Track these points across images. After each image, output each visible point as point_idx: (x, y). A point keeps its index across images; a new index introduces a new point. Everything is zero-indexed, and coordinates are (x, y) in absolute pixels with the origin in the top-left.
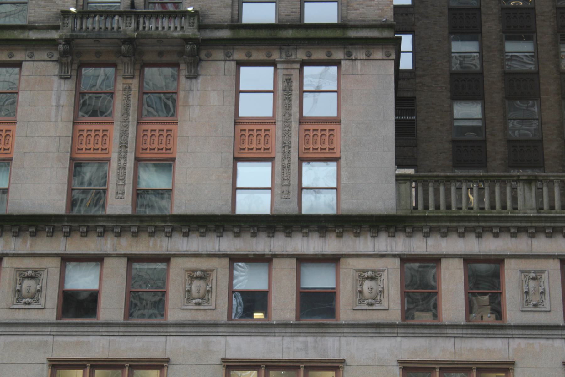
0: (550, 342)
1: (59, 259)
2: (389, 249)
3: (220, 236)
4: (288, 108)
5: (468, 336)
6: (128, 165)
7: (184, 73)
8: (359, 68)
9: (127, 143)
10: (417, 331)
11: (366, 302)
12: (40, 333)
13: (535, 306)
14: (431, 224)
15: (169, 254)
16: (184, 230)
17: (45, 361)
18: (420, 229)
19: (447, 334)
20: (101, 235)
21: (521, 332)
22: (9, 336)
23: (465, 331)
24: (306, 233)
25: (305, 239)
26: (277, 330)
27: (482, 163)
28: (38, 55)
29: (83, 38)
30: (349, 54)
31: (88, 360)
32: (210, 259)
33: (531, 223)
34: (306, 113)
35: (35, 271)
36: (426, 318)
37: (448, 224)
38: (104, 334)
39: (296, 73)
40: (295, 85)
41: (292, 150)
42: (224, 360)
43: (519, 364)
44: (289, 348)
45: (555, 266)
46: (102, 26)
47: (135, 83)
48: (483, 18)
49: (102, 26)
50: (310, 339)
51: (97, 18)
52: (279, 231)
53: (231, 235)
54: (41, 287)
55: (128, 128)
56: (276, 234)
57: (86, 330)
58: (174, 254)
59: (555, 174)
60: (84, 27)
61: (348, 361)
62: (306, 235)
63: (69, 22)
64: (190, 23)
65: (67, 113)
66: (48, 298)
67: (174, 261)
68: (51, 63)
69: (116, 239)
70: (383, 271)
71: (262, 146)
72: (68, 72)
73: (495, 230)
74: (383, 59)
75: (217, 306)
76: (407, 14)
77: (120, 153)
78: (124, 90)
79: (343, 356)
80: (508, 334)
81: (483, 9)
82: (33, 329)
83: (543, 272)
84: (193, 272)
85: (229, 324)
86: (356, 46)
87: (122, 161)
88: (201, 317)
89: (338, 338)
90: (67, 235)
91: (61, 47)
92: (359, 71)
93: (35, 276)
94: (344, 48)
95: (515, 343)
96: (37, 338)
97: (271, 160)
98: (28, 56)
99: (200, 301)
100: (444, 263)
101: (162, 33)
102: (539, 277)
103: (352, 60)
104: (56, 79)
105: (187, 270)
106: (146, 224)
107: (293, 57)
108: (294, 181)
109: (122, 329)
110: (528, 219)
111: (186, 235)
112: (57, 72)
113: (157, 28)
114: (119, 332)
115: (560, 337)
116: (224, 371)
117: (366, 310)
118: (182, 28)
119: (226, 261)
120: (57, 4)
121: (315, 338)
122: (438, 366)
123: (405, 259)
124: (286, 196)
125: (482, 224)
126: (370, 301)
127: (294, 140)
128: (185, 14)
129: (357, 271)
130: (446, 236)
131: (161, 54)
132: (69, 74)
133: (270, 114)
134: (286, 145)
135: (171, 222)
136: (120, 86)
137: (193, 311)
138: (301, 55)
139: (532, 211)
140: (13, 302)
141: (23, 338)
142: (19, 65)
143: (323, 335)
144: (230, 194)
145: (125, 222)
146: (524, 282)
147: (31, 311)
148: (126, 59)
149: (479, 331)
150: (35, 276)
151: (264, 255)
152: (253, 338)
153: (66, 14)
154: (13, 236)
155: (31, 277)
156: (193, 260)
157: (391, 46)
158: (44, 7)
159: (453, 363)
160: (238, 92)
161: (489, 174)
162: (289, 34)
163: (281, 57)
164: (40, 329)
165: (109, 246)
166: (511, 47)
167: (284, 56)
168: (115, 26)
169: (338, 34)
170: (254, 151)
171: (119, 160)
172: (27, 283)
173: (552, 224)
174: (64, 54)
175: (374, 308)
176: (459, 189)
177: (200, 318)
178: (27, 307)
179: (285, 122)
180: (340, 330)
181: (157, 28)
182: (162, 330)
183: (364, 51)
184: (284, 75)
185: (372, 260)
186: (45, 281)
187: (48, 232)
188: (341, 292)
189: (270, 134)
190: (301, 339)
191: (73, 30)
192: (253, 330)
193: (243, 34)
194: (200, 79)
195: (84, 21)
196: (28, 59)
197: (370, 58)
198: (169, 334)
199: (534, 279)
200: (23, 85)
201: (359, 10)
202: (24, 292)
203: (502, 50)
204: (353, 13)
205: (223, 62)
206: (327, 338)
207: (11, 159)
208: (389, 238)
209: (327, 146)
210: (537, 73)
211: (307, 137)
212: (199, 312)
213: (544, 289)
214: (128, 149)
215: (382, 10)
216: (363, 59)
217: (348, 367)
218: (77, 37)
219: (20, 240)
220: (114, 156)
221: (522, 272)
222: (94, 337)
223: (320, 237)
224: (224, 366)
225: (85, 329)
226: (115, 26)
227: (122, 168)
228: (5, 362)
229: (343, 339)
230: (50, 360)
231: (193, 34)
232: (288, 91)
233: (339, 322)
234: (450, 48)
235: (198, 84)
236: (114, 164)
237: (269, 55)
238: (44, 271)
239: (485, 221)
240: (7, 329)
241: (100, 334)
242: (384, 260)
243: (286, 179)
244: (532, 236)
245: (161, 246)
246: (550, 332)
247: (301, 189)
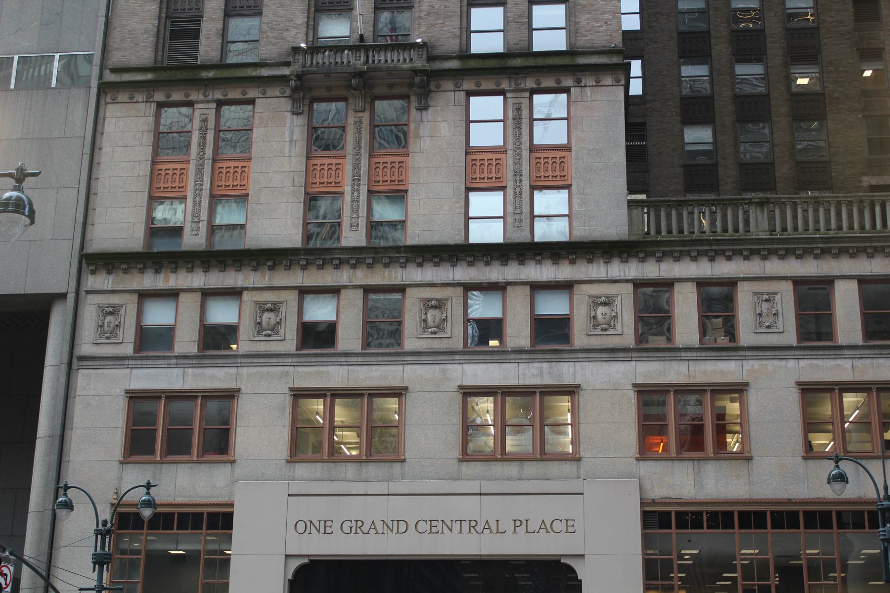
0: (784, 362)
1: (297, 291)
2: (622, 274)
3: (454, 265)
4: (518, 137)
5: (702, 358)
6: (361, 198)
7: (414, 104)
8: (589, 95)
9: (360, 176)
10: (651, 354)
11: (600, 327)
12: (281, 364)
13: (768, 327)
14: (664, 249)
15: (404, 285)
16: (418, 261)
17: (287, 391)
18: (653, 254)
19: (681, 357)
20: (337, 267)
21: (754, 353)
22: (251, 368)
23: (699, 354)
24: (539, 261)
25: (538, 266)
26: (512, 357)
27: (714, 187)
28: (271, 92)
29: (314, 73)
30: (578, 81)
31: (328, 389)
32: (444, 288)
33: (764, 245)
34: (536, 141)
35: (274, 304)
36: (660, 342)
37: (681, 248)
38: (342, 363)
39: (526, 102)
40: (525, 113)
41: (523, 178)
42: (461, 387)
43: (752, 385)
44: (524, 374)
45: (787, 288)
46: (332, 61)
47: (366, 116)
48: (713, 41)
49: (332, 61)
50: (545, 365)
51: (327, 53)
52: (512, 259)
53: (464, 264)
54: (281, 319)
55: (360, 161)
56: (509, 262)
57: (325, 360)
58: (409, 284)
59: (787, 196)
60: (314, 62)
61: (584, 386)
62: (539, 262)
63: (300, 58)
64: (419, 55)
65: (300, 148)
66: (287, 330)
67: (409, 291)
68: (283, 99)
69: (352, 270)
71: (493, 175)
72: (300, 108)
73: (728, 253)
74: (612, 85)
75: (453, 334)
76: (635, 40)
77: (353, 186)
78: (355, 123)
79: (578, 381)
80: (741, 356)
81: (712, 33)
82: (274, 360)
83: (776, 294)
84: (429, 301)
85: (465, 352)
86: (585, 73)
87: (356, 194)
88: (436, 345)
89: (573, 363)
90: (304, 268)
91: (293, 83)
92: (589, 97)
93: (274, 308)
94: (574, 75)
95: (748, 365)
96: (279, 368)
97: (503, 189)
98: (261, 93)
99: (436, 329)
100: (677, 287)
101: (391, 65)
102: (772, 299)
103: (581, 86)
104: (288, 115)
105: (422, 300)
106: (380, 255)
107: (522, 86)
108: (526, 209)
109: (360, 359)
110: (760, 241)
111: (420, 265)
112: (289, 108)
113: (386, 61)
114: (357, 362)
115: (793, 357)
116: (461, 398)
117: (600, 335)
118: (411, 60)
119: (460, 290)
120: (288, 41)
121: (550, 363)
122: (672, 389)
123: (638, 284)
124: (518, 224)
126: (604, 326)
127: (525, 168)
128: (414, 46)
129: (590, 296)
130: (679, 261)
131: (391, 86)
132: (302, 109)
133: (500, 143)
134: (518, 174)
135: (405, 253)
136: (351, 120)
137: (429, 340)
138: (530, 83)
139: (765, 234)
140: (254, 334)
141: (265, 369)
142: (252, 102)
143: (558, 361)
144: (463, 224)
145: (361, 254)
146: (757, 304)
147: (272, 342)
148: (357, 93)
149: (713, 354)
150: (274, 308)
151: (497, 283)
152: (488, 365)
153: (296, 50)
154: (252, 270)
155: (271, 310)
156: (428, 289)
157: (620, 72)
158: (275, 44)
159: (687, 385)
160: (468, 122)
161: (721, 197)
162: (518, 62)
163: (510, 85)
164: (281, 360)
165: (345, 277)
166: (741, 70)
167: (513, 84)
168: (345, 61)
169: (567, 61)
170: (486, 180)
171: (353, 193)
172: (266, 316)
173: (785, 246)
174: (295, 90)
175: (608, 333)
176: (691, 213)
177: (436, 347)
178: (268, 338)
179: (516, 151)
180: (575, 355)
181: (386, 61)
182: (399, 358)
183: (594, 77)
184: (514, 104)
185: (605, 285)
186: (284, 313)
187: (286, 266)
188: (575, 318)
189: (501, 163)
190: (536, 365)
191: (304, 66)
192: (489, 357)
193: (472, 64)
194: (431, 110)
195: (315, 57)
196: (261, 95)
197: (599, 85)
198: (406, 363)
199: (766, 301)
200: (256, 122)
201: (587, 36)
202: (264, 324)
203: (732, 73)
204: (581, 40)
205: (453, 93)
206: (562, 363)
207: (248, 195)
208: (622, 264)
209: (558, 173)
210: (767, 96)
211: (539, 165)
212: (435, 340)
213: (777, 310)
214: (361, 182)
215: (611, 36)
216: (592, 86)
217: (583, 391)
218: (308, 73)
219: (258, 275)
220: (348, 189)
221: (755, 294)
222: (333, 367)
223: (553, 264)
224: (461, 393)
225: (325, 359)
226: (345, 61)
227: (355, 200)
228: (248, 392)
229: (578, 364)
230: (291, 390)
231: (423, 66)
232: (518, 119)
233: (574, 348)
234: (680, 72)
235: (429, 115)
236: (348, 197)
237: (498, 84)
238: (282, 303)
239: (718, 245)
240: (250, 360)
241: (339, 363)
242: (617, 285)
243: (518, 209)
244: (765, 258)
245: (396, 277)
246: (783, 353)
247: (533, 217)
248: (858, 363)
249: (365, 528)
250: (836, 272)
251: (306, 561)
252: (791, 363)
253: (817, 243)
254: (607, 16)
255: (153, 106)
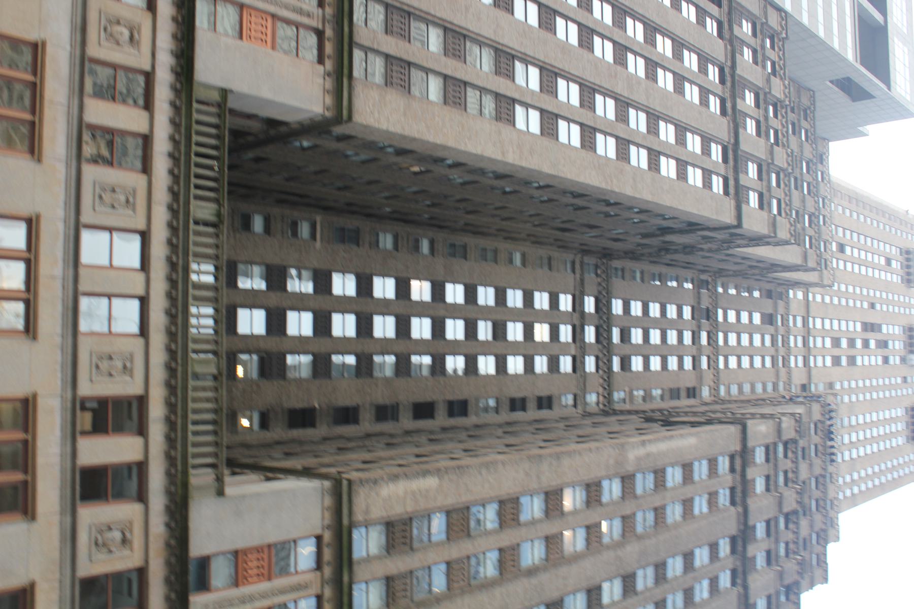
0: (62, 204)
13: (101, 197)
37: (183, 123)
59: (225, 241)
70: (139, 51)
83: (134, 210)
95: (61, 169)
103: (325, 75)
123: (149, 77)
125: (183, 158)
159: (42, 97)
221: (134, 191)
244: (170, 208)
248: (58, 284)
250: (153, 275)
252: (60, 213)
253: (183, 259)
254: (376, 115)
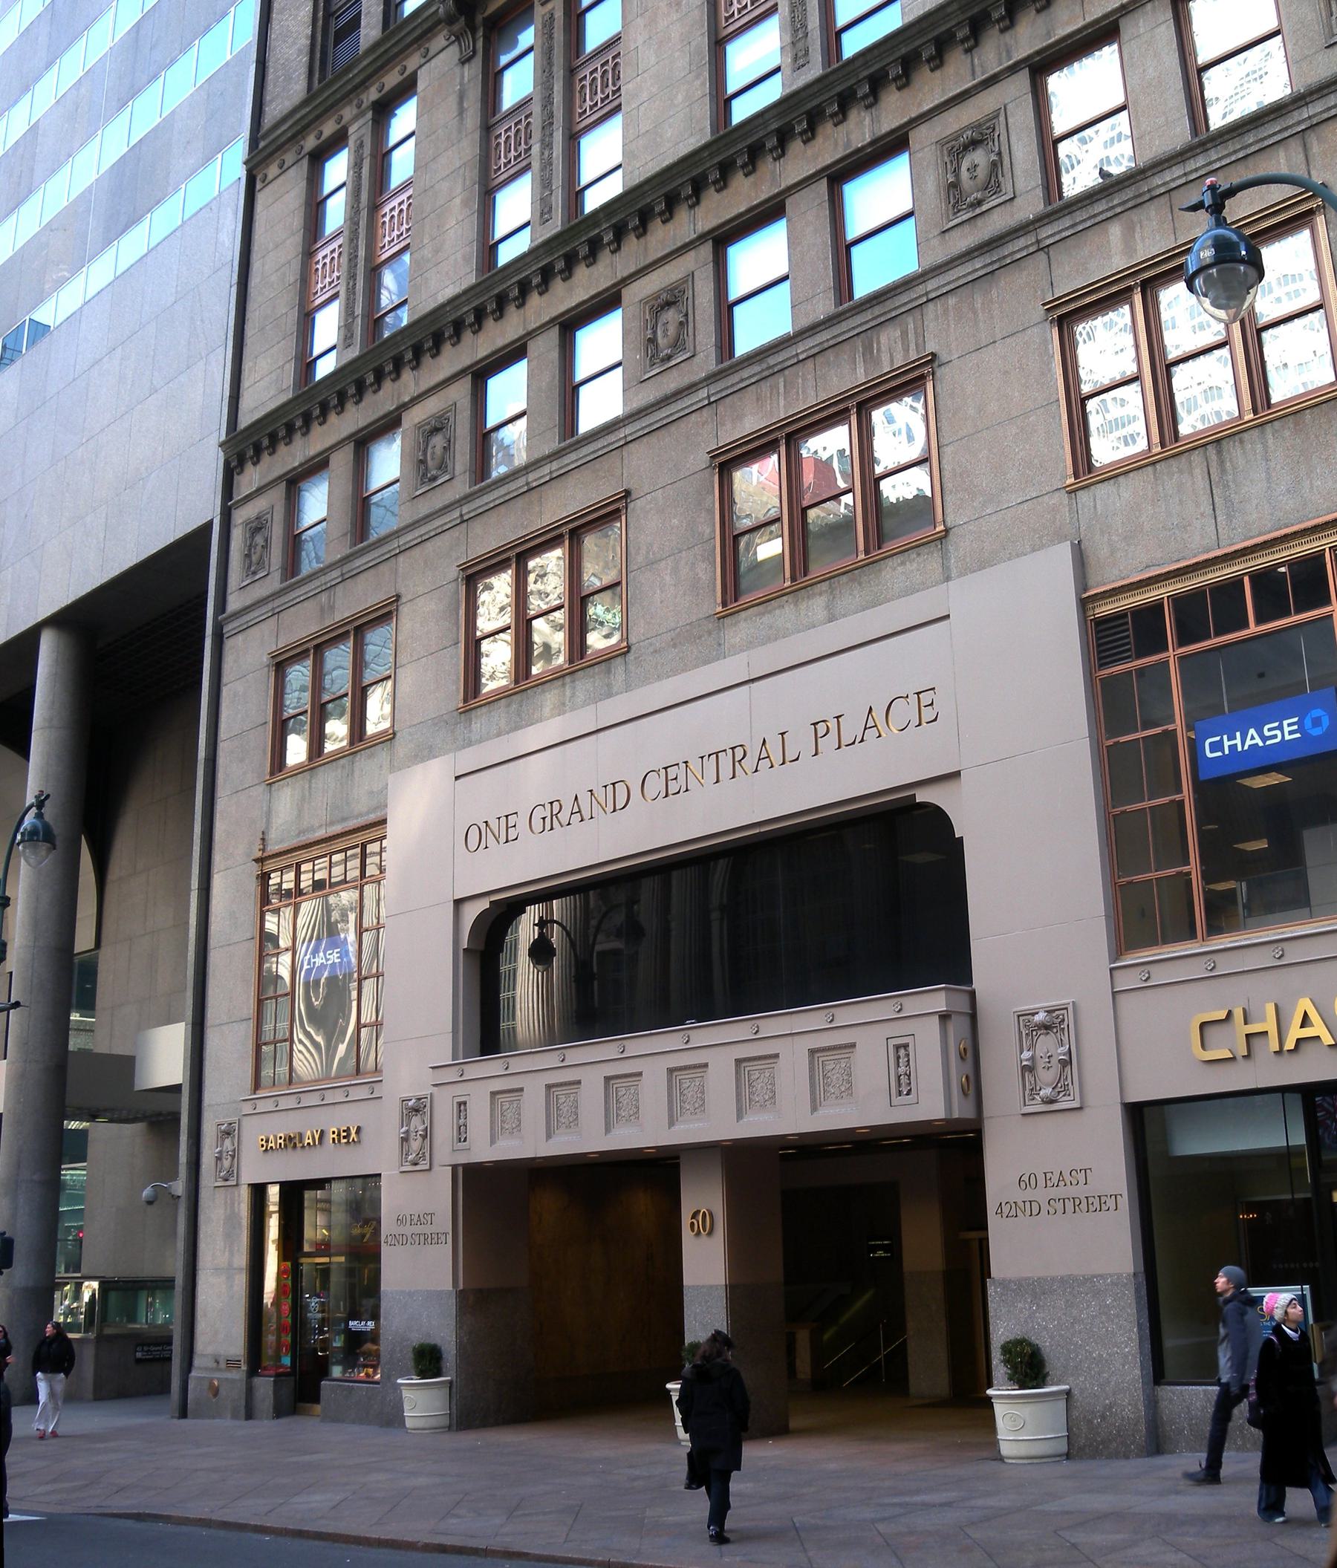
70: (997, 116)
140: (417, 484)
175: (984, 208)
214: (555, 127)
249: (564, 817)
251: (484, 905)
255: (305, 162)
